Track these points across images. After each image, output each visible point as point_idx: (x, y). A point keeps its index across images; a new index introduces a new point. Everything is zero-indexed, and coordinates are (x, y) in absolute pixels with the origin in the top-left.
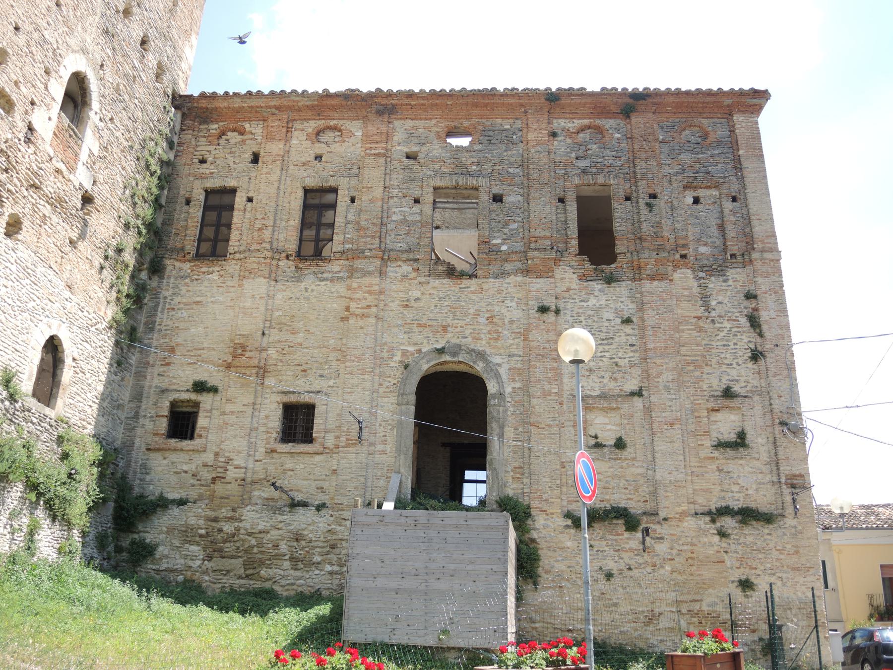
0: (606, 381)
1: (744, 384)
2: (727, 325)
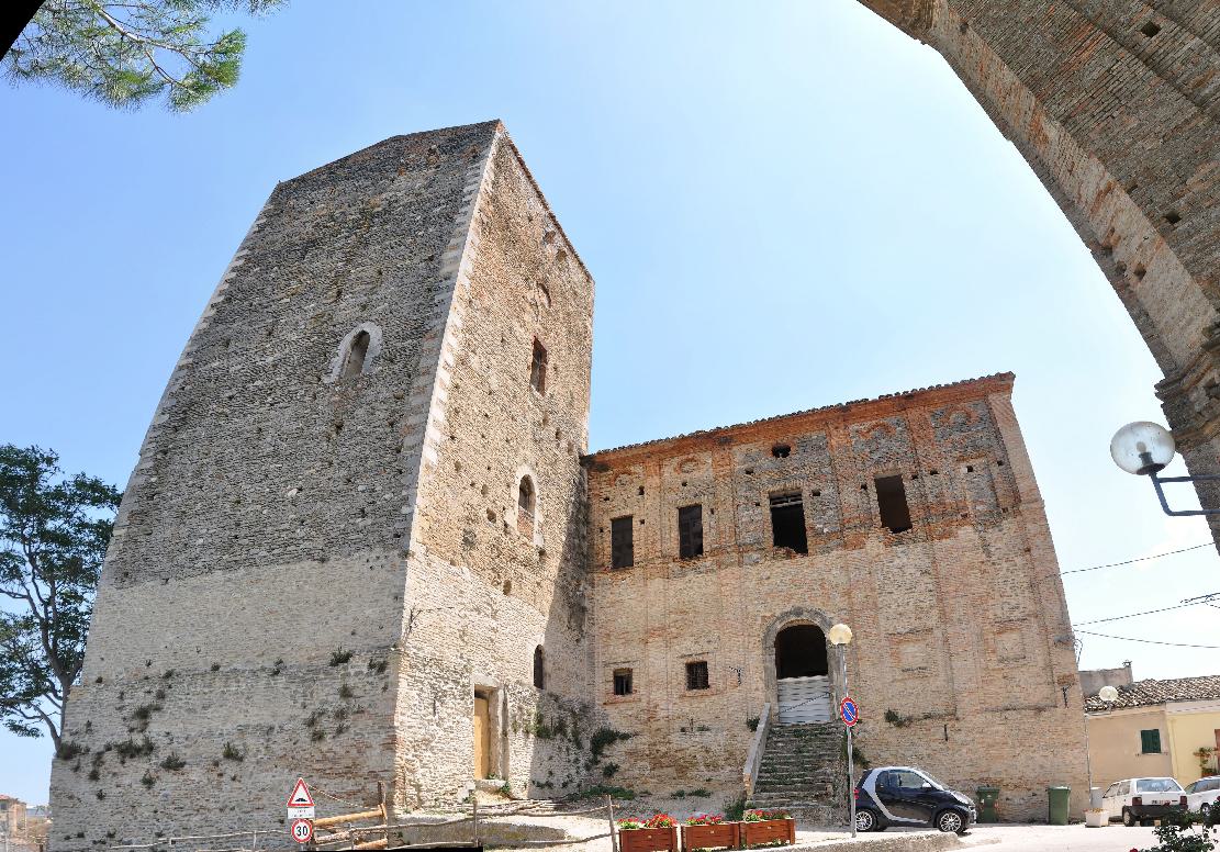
0: (912, 620)
1: (1022, 610)
2: (1005, 565)
